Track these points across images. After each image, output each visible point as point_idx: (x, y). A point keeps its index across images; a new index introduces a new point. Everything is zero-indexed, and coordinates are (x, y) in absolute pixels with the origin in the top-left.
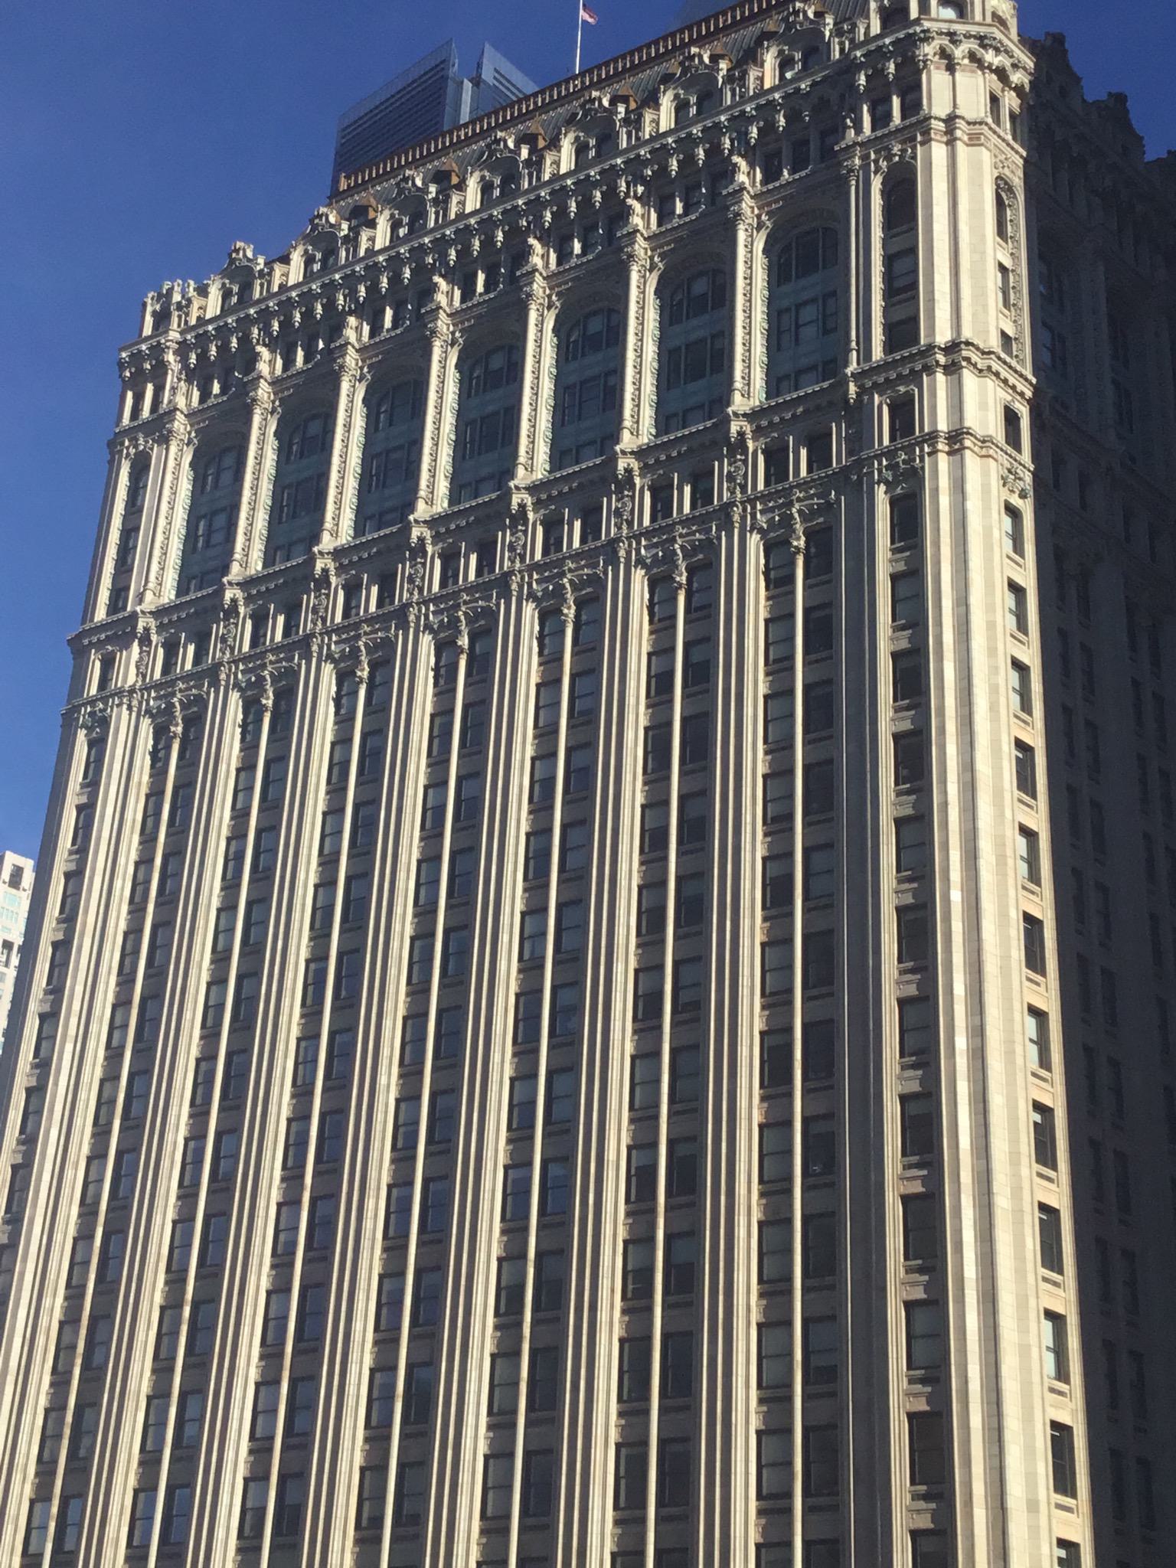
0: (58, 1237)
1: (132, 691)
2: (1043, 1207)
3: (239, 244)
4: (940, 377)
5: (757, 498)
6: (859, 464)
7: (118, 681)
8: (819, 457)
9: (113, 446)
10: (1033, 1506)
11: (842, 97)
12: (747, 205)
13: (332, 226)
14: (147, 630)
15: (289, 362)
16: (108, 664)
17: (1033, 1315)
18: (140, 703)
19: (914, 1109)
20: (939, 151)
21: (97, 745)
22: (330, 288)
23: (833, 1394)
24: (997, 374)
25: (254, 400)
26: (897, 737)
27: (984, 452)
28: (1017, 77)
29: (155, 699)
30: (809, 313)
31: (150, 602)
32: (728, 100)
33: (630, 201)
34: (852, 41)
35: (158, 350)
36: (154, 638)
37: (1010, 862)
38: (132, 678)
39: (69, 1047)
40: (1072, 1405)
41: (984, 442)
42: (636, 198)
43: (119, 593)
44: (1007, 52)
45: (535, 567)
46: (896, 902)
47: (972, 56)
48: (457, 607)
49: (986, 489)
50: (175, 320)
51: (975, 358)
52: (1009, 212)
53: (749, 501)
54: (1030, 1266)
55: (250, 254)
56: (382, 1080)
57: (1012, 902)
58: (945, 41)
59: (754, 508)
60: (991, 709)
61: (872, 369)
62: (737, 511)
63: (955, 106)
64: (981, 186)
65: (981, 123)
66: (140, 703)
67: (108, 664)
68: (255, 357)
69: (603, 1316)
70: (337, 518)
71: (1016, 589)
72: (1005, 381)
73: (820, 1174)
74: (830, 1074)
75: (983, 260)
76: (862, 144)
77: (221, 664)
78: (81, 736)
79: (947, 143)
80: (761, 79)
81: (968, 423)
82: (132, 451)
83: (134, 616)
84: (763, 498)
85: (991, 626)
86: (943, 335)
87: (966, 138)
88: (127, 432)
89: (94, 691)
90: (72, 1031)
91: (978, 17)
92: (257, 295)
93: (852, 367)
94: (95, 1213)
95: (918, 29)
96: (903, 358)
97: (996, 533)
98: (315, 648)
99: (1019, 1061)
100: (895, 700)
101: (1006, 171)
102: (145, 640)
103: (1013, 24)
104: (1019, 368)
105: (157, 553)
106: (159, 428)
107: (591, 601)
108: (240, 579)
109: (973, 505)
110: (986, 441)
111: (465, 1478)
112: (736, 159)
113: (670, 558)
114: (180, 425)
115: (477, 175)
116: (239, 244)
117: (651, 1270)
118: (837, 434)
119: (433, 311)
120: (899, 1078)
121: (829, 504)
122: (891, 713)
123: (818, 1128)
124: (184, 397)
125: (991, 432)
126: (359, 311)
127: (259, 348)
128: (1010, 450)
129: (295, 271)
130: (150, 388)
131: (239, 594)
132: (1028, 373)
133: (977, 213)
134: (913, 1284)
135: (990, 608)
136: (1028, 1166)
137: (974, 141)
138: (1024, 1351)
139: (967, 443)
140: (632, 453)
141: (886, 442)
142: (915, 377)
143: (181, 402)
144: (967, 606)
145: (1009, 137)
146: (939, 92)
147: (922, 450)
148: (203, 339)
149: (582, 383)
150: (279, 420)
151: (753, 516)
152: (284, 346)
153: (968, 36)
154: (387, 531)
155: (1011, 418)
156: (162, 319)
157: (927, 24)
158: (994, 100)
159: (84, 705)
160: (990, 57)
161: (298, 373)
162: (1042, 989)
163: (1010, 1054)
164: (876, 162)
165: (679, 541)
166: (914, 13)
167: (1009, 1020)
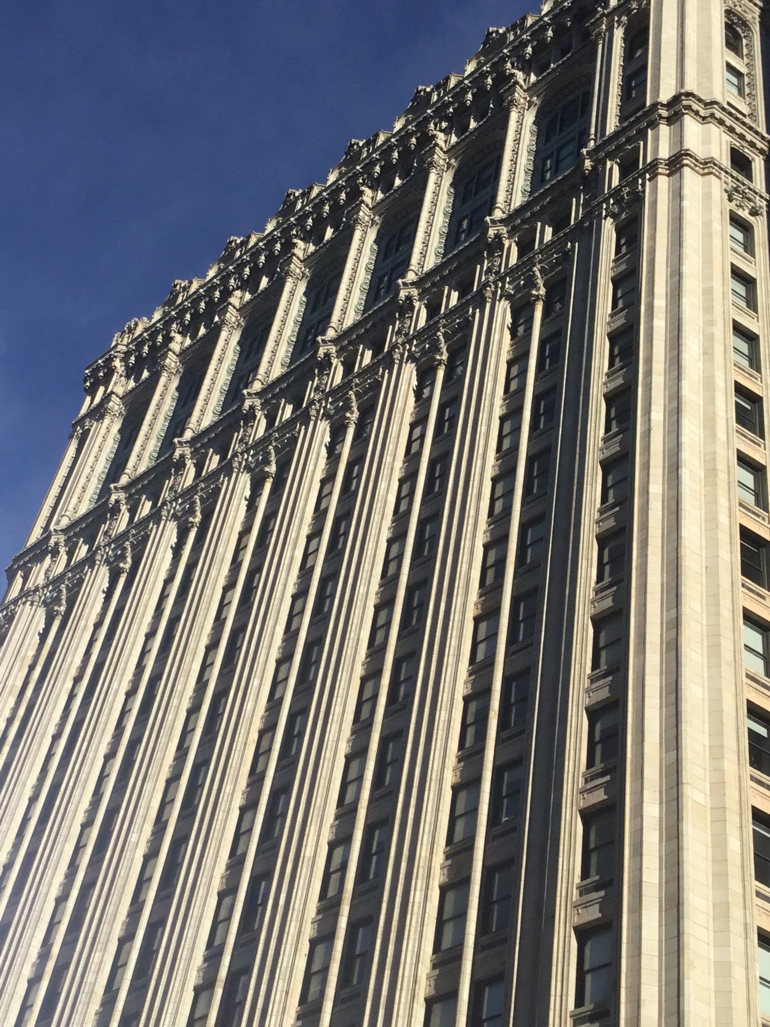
14: (57, 544)
27: (706, 171)
41: (706, 163)
42: (441, 131)
51: (695, 107)
52: (744, 42)
60: (705, 353)
76: (607, 16)
81: (687, 145)
86: (665, 96)
120: (588, 691)
132: (762, 130)
134: (586, 905)
142: (642, 135)
144: (680, 274)
150: (181, 379)
155: (740, 162)
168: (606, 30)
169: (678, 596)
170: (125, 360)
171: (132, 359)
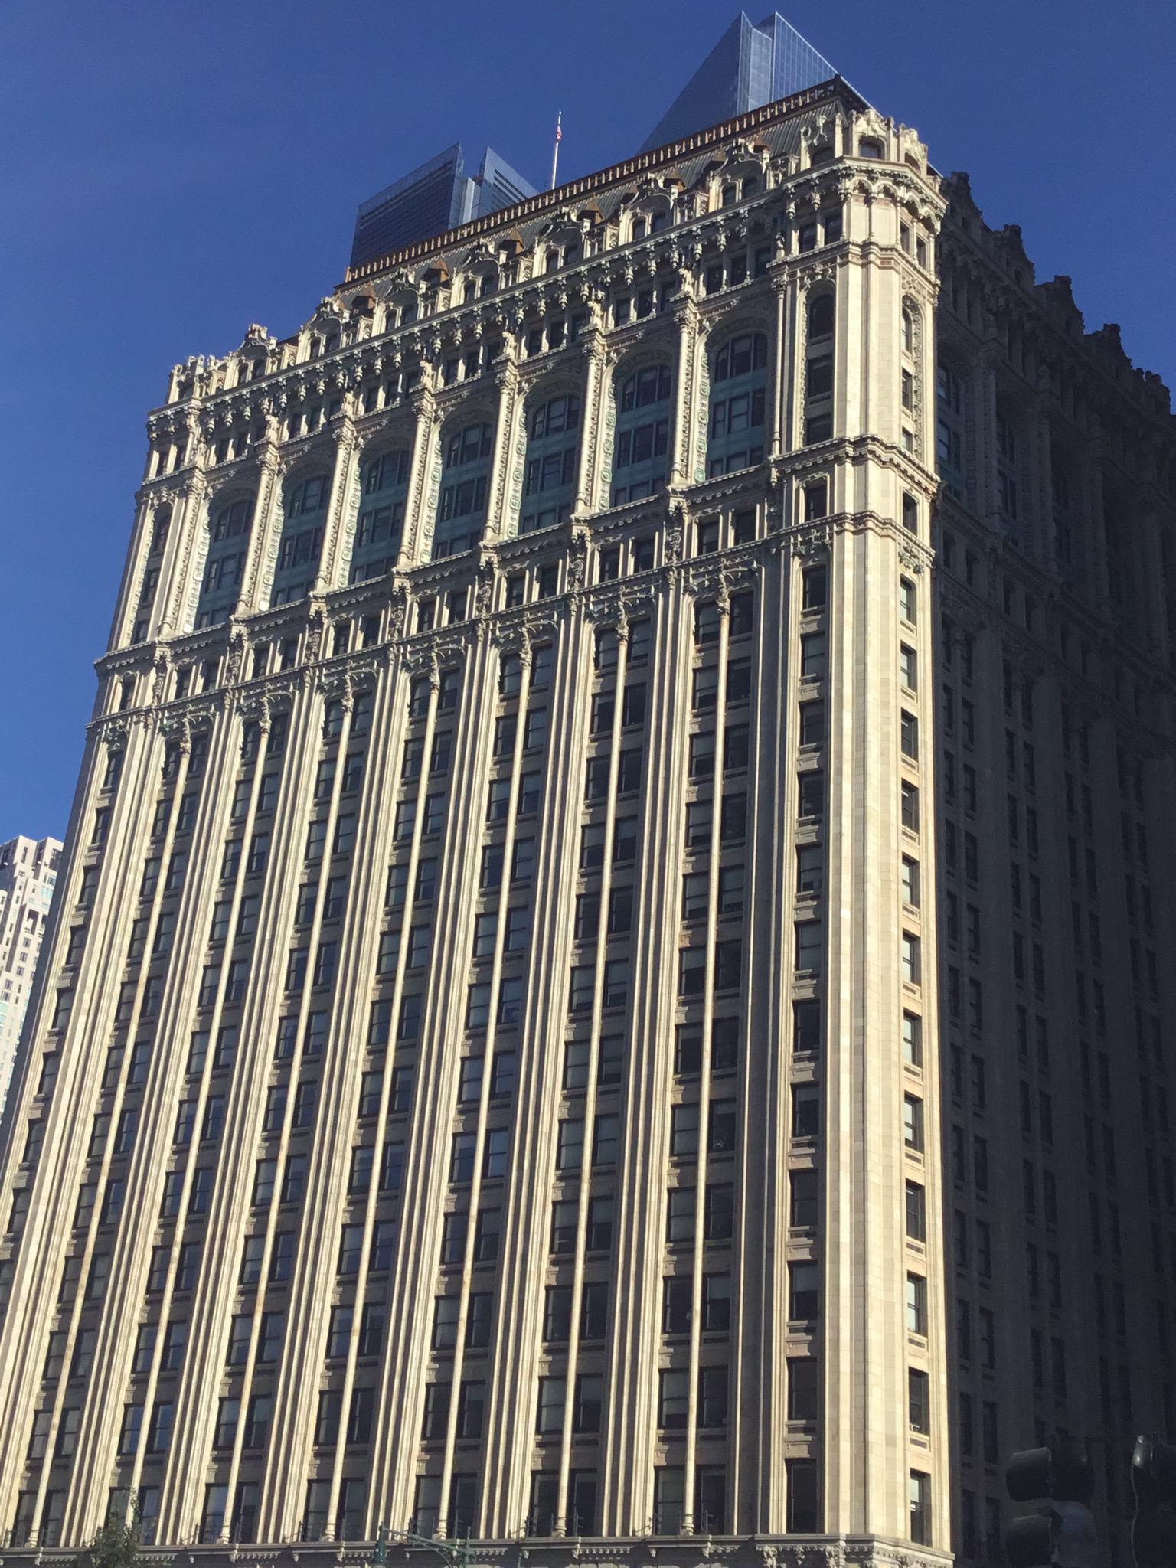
0: (66, 1184)
1: (148, 711)
2: (910, 1184)
3: (255, 326)
4: (849, 466)
5: (690, 565)
6: (778, 538)
7: (135, 703)
8: (744, 529)
9: (140, 496)
10: (891, 1441)
11: (775, 221)
12: (691, 312)
13: (335, 314)
14: (163, 658)
15: (294, 430)
16: (128, 686)
17: (897, 1276)
18: (155, 722)
19: (804, 1096)
20: (855, 272)
21: (117, 758)
22: (332, 367)
23: (724, 1340)
24: (898, 466)
25: (263, 463)
26: (801, 776)
28: (924, 211)
29: (168, 718)
30: (741, 407)
31: (167, 634)
32: (678, 220)
33: (591, 304)
34: (785, 174)
35: (182, 415)
36: (169, 666)
37: (894, 886)
38: (149, 700)
39: (82, 1019)
40: (928, 1355)
42: (597, 301)
43: (141, 624)
44: (916, 189)
45: (499, 616)
46: (795, 917)
47: (886, 191)
48: (431, 648)
49: (885, 564)
50: (197, 390)
51: (879, 451)
52: (913, 326)
53: (683, 566)
54: (896, 1234)
55: (264, 335)
56: (351, 1056)
57: (894, 921)
58: (864, 178)
59: (687, 572)
60: (882, 754)
61: (791, 457)
62: (673, 574)
63: (870, 234)
64: (890, 303)
65: (892, 250)
66: (155, 722)
67: (128, 686)
68: (265, 425)
69: (532, 1266)
70: (330, 567)
71: (908, 651)
72: (905, 472)
73: (725, 1149)
74: (733, 1064)
75: (890, 368)
76: (789, 264)
77: (226, 690)
78: (104, 748)
79: (863, 266)
80: (707, 203)
81: (870, 508)
82: (156, 502)
83: (152, 647)
84: (695, 564)
85: (885, 682)
86: (853, 432)
87: (878, 262)
88: (156, 486)
89: (116, 709)
90: (85, 1005)
91: (893, 158)
92: (268, 372)
93: (775, 455)
94: (100, 1164)
95: (841, 166)
96: (818, 449)
97: (892, 602)
98: (307, 679)
99: (895, 1058)
100: (802, 743)
101: (912, 291)
102: (161, 668)
103: (924, 163)
104: (917, 461)
105: (174, 591)
106: (180, 483)
107: (545, 649)
108: (245, 617)
109: (873, 578)
110: (886, 523)
111: (408, 1403)
112: (682, 271)
113: (614, 614)
114: (198, 481)
115: (461, 275)
116: (255, 326)
117: (574, 1228)
118: (762, 512)
119: (419, 391)
120: (792, 1069)
121: (751, 572)
122: (797, 755)
123: (722, 1110)
124: (202, 457)
125: (891, 514)
126: (356, 387)
127: (268, 417)
128: (907, 531)
129: (303, 352)
130: (173, 451)
131: (244, 631)
133: (886, 327)
134: (797, 1247)
135: (885, 667)
136: (899, 1150)
137: (886, 264)
138: (889, 1306)
139: (870, 524)
140: (585, 521)
141: (802, 520)
143: (200, 461)
144: (865, 664)
145: (916, 262)
146: (856, 221)
147: (831, 529)
148: (221, 406)
149: (546, 459)
151: (687, 580)
152: (291, 415)
153: (884, 174)
154: (373, 580)
156: (186, 388)
157: (848, 163)
158: (904, 229)
159: (107, 721)
160: (901, 192)
161: (302, 441)
162: (917, 996)
163: (886, 1051)
164: (801, 279)
165: (623, 599)
166: (838, 152)
167: (887, 1021)
168: (789, 283)
169: (864, 1007)
170: (202, 421)
171: (212, 425)
